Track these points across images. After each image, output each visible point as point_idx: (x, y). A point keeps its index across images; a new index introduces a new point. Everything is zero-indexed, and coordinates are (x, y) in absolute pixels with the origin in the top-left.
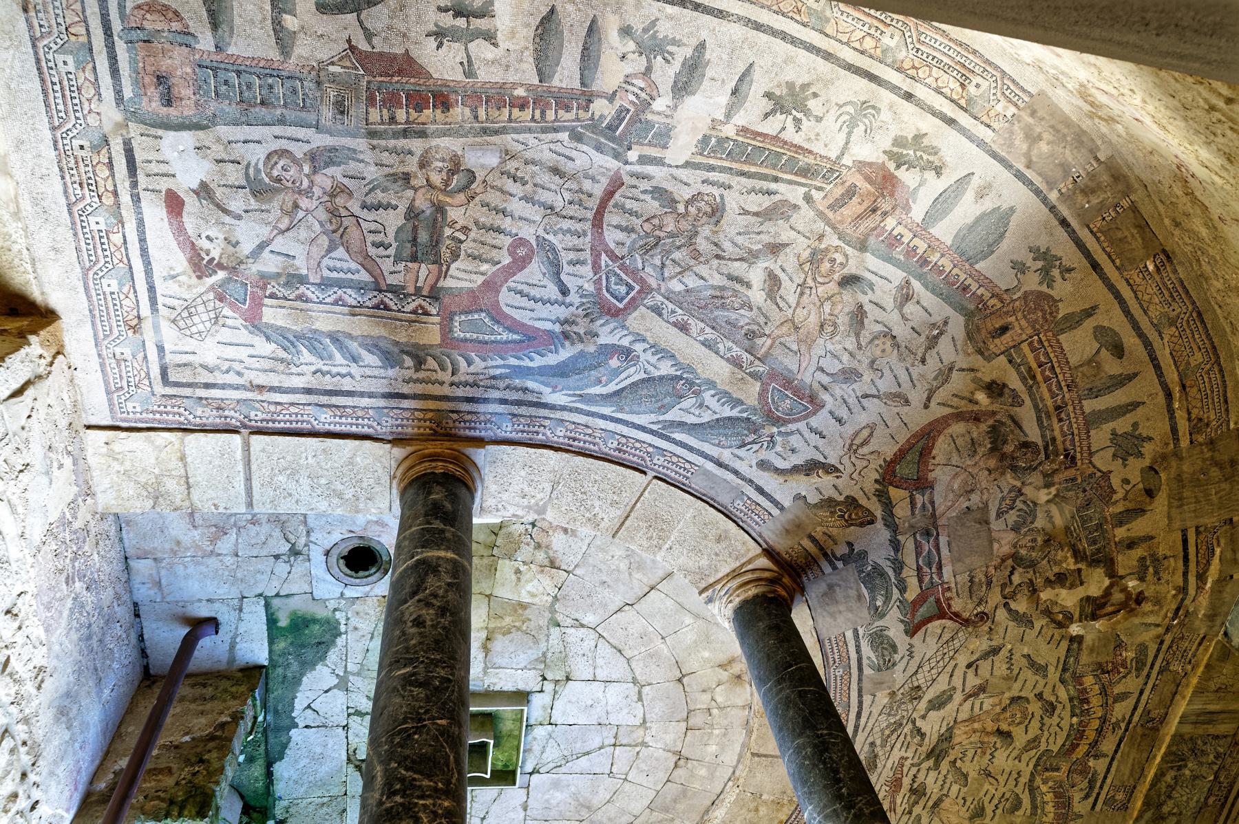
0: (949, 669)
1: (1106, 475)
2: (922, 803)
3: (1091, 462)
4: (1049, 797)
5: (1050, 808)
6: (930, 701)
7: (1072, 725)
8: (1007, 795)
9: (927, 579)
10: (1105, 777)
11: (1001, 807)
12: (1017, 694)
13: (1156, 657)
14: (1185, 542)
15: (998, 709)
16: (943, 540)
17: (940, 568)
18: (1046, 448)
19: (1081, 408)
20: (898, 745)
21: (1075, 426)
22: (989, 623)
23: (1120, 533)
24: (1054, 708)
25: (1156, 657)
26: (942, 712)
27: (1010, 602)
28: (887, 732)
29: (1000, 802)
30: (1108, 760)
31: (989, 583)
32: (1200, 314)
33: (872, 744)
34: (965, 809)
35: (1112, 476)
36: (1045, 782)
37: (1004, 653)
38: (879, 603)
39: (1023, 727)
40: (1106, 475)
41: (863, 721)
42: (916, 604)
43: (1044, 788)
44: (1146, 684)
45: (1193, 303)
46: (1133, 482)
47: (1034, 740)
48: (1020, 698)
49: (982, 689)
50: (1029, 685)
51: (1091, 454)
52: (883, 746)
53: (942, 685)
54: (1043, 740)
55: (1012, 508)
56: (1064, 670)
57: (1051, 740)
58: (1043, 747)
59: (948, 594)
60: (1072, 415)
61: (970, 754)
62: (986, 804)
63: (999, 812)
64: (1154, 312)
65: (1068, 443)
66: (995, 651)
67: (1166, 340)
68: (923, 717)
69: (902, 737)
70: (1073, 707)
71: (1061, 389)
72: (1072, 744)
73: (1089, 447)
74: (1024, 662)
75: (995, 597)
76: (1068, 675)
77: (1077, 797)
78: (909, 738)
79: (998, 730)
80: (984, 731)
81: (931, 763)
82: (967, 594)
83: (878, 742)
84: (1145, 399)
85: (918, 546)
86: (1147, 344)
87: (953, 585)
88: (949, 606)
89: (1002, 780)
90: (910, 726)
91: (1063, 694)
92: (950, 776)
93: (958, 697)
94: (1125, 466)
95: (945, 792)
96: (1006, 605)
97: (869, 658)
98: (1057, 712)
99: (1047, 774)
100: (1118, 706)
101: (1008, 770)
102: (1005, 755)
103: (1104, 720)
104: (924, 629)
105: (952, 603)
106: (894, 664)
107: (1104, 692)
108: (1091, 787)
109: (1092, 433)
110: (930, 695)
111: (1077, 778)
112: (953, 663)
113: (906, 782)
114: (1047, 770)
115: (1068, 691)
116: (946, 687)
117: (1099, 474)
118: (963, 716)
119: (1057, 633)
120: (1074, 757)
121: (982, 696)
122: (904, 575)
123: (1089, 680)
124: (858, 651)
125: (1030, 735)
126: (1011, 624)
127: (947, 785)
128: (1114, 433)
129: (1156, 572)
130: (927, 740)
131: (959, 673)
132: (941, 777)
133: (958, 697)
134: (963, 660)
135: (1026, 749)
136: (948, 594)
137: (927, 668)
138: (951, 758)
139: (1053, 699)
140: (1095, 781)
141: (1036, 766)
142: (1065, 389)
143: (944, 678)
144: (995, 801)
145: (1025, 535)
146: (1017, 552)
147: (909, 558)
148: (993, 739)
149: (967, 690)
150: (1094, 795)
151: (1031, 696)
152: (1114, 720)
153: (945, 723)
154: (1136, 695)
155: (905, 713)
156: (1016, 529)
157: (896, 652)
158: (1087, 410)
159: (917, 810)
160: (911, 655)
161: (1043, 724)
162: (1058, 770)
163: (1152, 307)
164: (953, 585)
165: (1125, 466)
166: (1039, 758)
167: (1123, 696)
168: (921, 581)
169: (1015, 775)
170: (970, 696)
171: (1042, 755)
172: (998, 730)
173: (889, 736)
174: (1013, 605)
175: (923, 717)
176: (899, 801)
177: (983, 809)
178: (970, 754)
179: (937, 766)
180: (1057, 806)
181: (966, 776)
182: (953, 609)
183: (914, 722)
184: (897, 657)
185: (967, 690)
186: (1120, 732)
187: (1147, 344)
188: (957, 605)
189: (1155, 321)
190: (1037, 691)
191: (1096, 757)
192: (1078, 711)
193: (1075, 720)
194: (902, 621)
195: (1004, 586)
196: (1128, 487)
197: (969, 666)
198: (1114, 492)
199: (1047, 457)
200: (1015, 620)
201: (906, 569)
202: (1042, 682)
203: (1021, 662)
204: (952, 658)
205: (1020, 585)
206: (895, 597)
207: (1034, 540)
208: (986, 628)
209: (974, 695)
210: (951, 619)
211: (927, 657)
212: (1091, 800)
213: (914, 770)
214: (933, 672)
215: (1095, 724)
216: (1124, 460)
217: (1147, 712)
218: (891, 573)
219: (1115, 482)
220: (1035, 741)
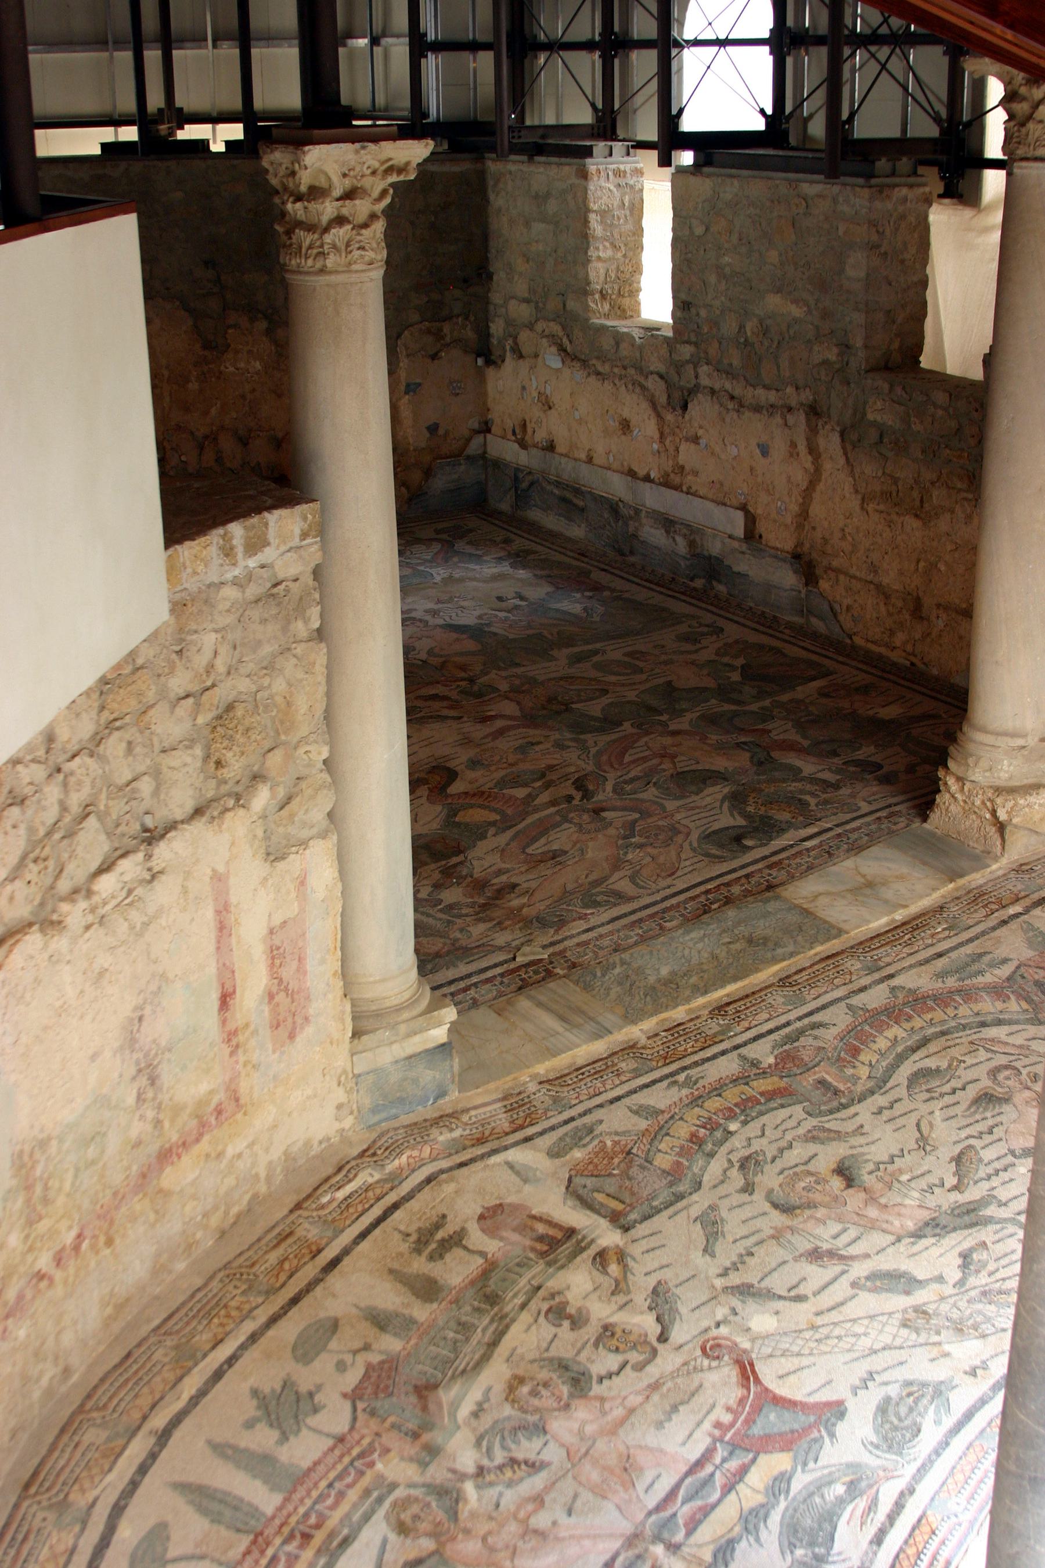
0: (834, 1316)
1: (354, 1396)
3: (352, 1428)
5: (882, 1043)
6: (907, 1293)
7: (745, 1123)
9: (733, 1464)
10: (770, 1032)
11: (947, 1088)
12: (775, 1214)
13: (553, 1128)
14: (363, 1235)
15: (821, 1213)
16: (652, 1501)
17: (699, 1464)
18: (380, 1500)
19: (280, 1509)
21: (315, 1494)
22: (714, 1332)
23: (421, 1312)
24: (747, 1158)
25: (553, 1128)
26: (905, 1266)
27: (653, 1339)
29: (942, 1095)
30: (743, 1051)
31: (655, 1386)
32: (27, 1486)
35: (348, 1389)
36: (856, 1079)
37: (735, 1279)
38: (839, 1489)
39: (811, 1167)
40: (354, 1396)
42: (786, 1442)
43: (864, 1072)
44: (601, 1106)
45: (16, 1506)
46: (336, 1358)
47: (814, 1139)
48: (775, 1206)
49: (815, 1255)
50: (747, 1212)
51: (341, 1440)
53: (868, 1302)
54: (801, 1131)
55: (513, 1462)
56: (680, 1197)
57: (792, 1123)
58: (812, 1122)
59: (727, 1418)
60: (302, 1510)
62: (964, 1105)
63: (955, 1083)
64: (60, 1540)
65: (349, 1480)
66: (745, 1291)
67: (95, 1493)
68: (940, 1279)
70: (721, 1143)
72: (769, 1100)
73: (332, 1449)
74: (719, 1247)
75: (667, 1361)
76: (681, 1188)
77: (829, 1035)
78: (991, 1267)
80: (872, 1199)
81: (990, 1211)
82: (698, 1399)
84: (201, 1444)
85: (693, 1525)
86: (118, 1510)
87: (707, 1425)
88: (742, 1402)
89: (913, 1118)
90: (972, 1281)
91: (716, 1167)
92: (981, 1174)
93: (859, 1270)
94: (319, 1387)
95: (1010, 1159)
96: (663, 1338)
97: (937, 1422)
98: (746, 1152)
99: (841, 1087)
100: (662, 1106)
101: (889, 1127)
102: (873, 1148)
103: (696, 1101)
104: (811, 1400)
105: (732, 1402)
106: (908, 1383)
107: (660, 1132)
108: (801, 1032)
109: (306, 1464)
110: (899, 1302)
111: (806, 1055)
112: (819, 1321)
114: (836, 1092)
115: (703, 1169)
116: (864, 1295)
117: (360, 1405)
118: (879, 1239)
119: (636, 1250)
120: (783, 1083)
121: (825, 1246)
122: (760, 1499)
123: (663, 1161)
124: (945, 1444)
125: (813, 1148)
126: (683, 1309)
127: (997, 1165)
128: (284, 1437)
129: (438, 1226)
130: (966, 1245)
131: (827, 1299)
132: (995, 1182)
133: (859, 1270)
134: (802, 1313)
135: (838, 1136)
136: (727, 1418)
137: (865, 1343)
138: (956, 1197)
139: (734, 1173)
140: (787, 1036)
141: (845, 1107)
142: (270, 1552)
143: (851, 1310)
145: (537, 1410)
146: (571, 1396)
147: (727, 1514)
148: (868, 1180)
149: (838, 1269)
150: (806, 1021)
151: (758, 1196)
152: (685, 1092)
154: (626, 1101)
156: (541, 1429)
157: (887, 1400)
158: (277, 1499)
160: (871, 1375)
161: (781, 1151)
162: (822, 1083)
163: (61, 1548)
164: (707, 1425)
165: (319, 1387)
166: (831, 1112)
167: (639, 1111)
168: (743, 1471)
169: (887, 1114)
170: (842, 1258)
171: (821, 1114)
172: (849, 1186)
174: (655, 1330)
177: (976, 1101)
179: (988, 1199)
180: (865, 1039)
182: (740, 1392)
183: (961, 1282)
184: (893, 1391)
185: (838, 1269)
186: (693, 1072)
187: (118, 1510)
188: (733, 1394)
189: (77, 1528)
190: (745, 1197)
191: (755, 1064)
192: (718, 1134)
193: (733, 1127)
194: (832, 1435)
195: (640, 1367)
196: (348, 1358)
197: (800, 1299)
198: (369, 1367)
199: (393, 1486)
200: (674, 1311)
201: (747, 1506)
202: (724, 1204)
203: (726, 1252)
204: (813, 1327)
205: (617, 1349)
206: (807, 1478)
207: (534, 1393)
208: (724, 1330)
209: (832, 1254)
210: (757, 1381)
211: (848, 1357)
212: (816, 1018)
215: (714, 1104)
216: (311, 1395)
217: (637, 1073)
218: (776, 1517)
219: (352, 1378)
220: (811, 1137)
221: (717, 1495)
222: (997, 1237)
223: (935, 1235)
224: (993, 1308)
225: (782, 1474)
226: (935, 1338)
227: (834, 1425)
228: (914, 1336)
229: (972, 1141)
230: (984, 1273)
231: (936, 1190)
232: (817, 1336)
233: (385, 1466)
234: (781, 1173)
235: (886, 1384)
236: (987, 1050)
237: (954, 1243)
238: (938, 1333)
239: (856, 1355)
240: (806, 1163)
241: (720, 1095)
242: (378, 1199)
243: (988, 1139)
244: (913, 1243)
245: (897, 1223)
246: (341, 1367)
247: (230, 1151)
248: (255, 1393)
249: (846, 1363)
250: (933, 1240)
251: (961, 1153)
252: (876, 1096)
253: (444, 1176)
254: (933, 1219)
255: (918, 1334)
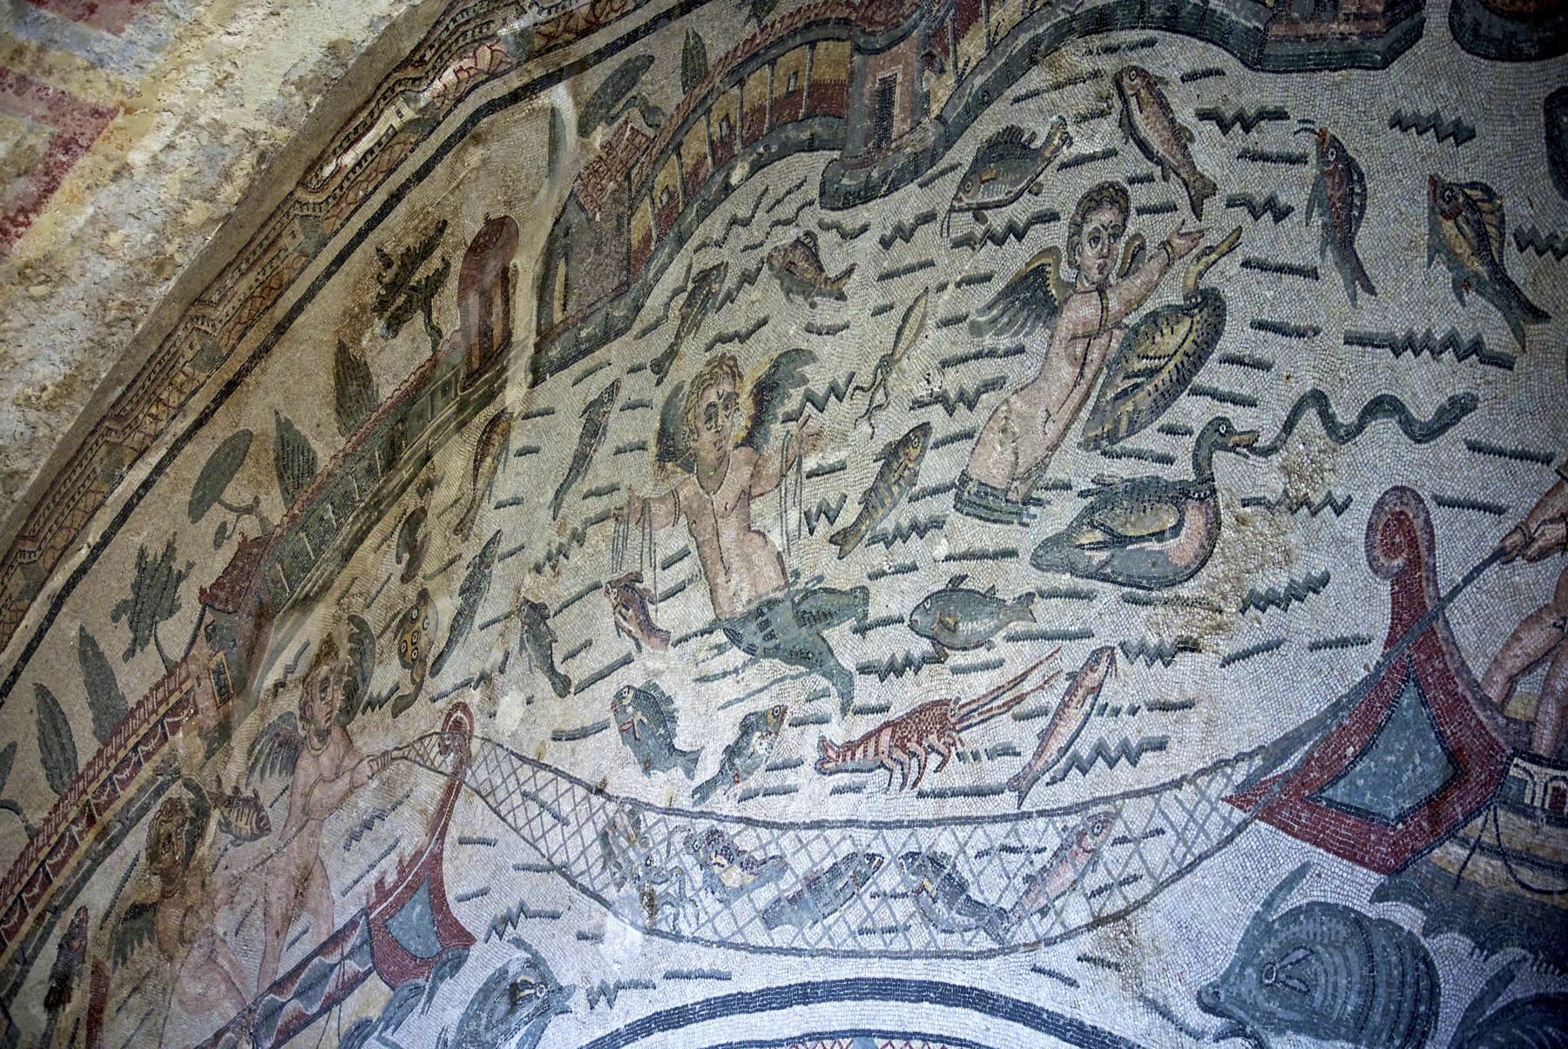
2: (980, 577)
3: (185, 659)
4: (972, 47)
6: (647, 766)
8: (963, 224)
9: (352, 966)
11: (997, 220)
18: (158, 793)
20: (775, 808)
24: (705, 277)
28: (734, 876)
33: (770, 918)
34: (1016, 370)
41: (694, 993)
52: (781, 864)
61: (816, 493)
62: (998, 285)
63: (1019, 212)
68: (691, 760)
69: (752, 809)
71: (63, 836)
79: (749, 441)
83: (764, 896)
92: (888, 525)
102: (825, 347)
113: (906, 695)
117: (209, 618)
127: (923, 510)
144: (985, 258)
153: (717, 665)
155: (678, 839)
159: (1016, 578)
173: (748, 864)
175: (691, 760)
176: (981, 683)
177: (1010, 291)
178: (816, 493)
181: (893, 454)
183: (704, 791)
213: (867, 690)
214: (566, 808)
221: (315, 1009)
222: (810, 709)
223: (751, 650)
224: (698, 876)
225: (368, 1021)
226: (611, 894)
227: (442, 979)
228: (596, 870)
229: (936, 414)
230: (739, 789)
231: (822, 527)
232: (529, 788)
233: (185, 736)
234: (709, 348)
235: (519, 943)
236: (1128, 126)
237: (757, 685)
238: (619, 885)
239: (533, 858)
240: (743, 338)
241: (772, 63)
242: (391, 171)
243: (964, 419)
244: (720, 649)
245: (735, 578)
246: (221, 534)
247: (137, 158)
248: (142, 554)
249: (517, 868)
250: (736, 656)
251: (905, 442)
252: (913, 187)
253: (484, 122)
254: (771, 604)
255: (604, 868)
